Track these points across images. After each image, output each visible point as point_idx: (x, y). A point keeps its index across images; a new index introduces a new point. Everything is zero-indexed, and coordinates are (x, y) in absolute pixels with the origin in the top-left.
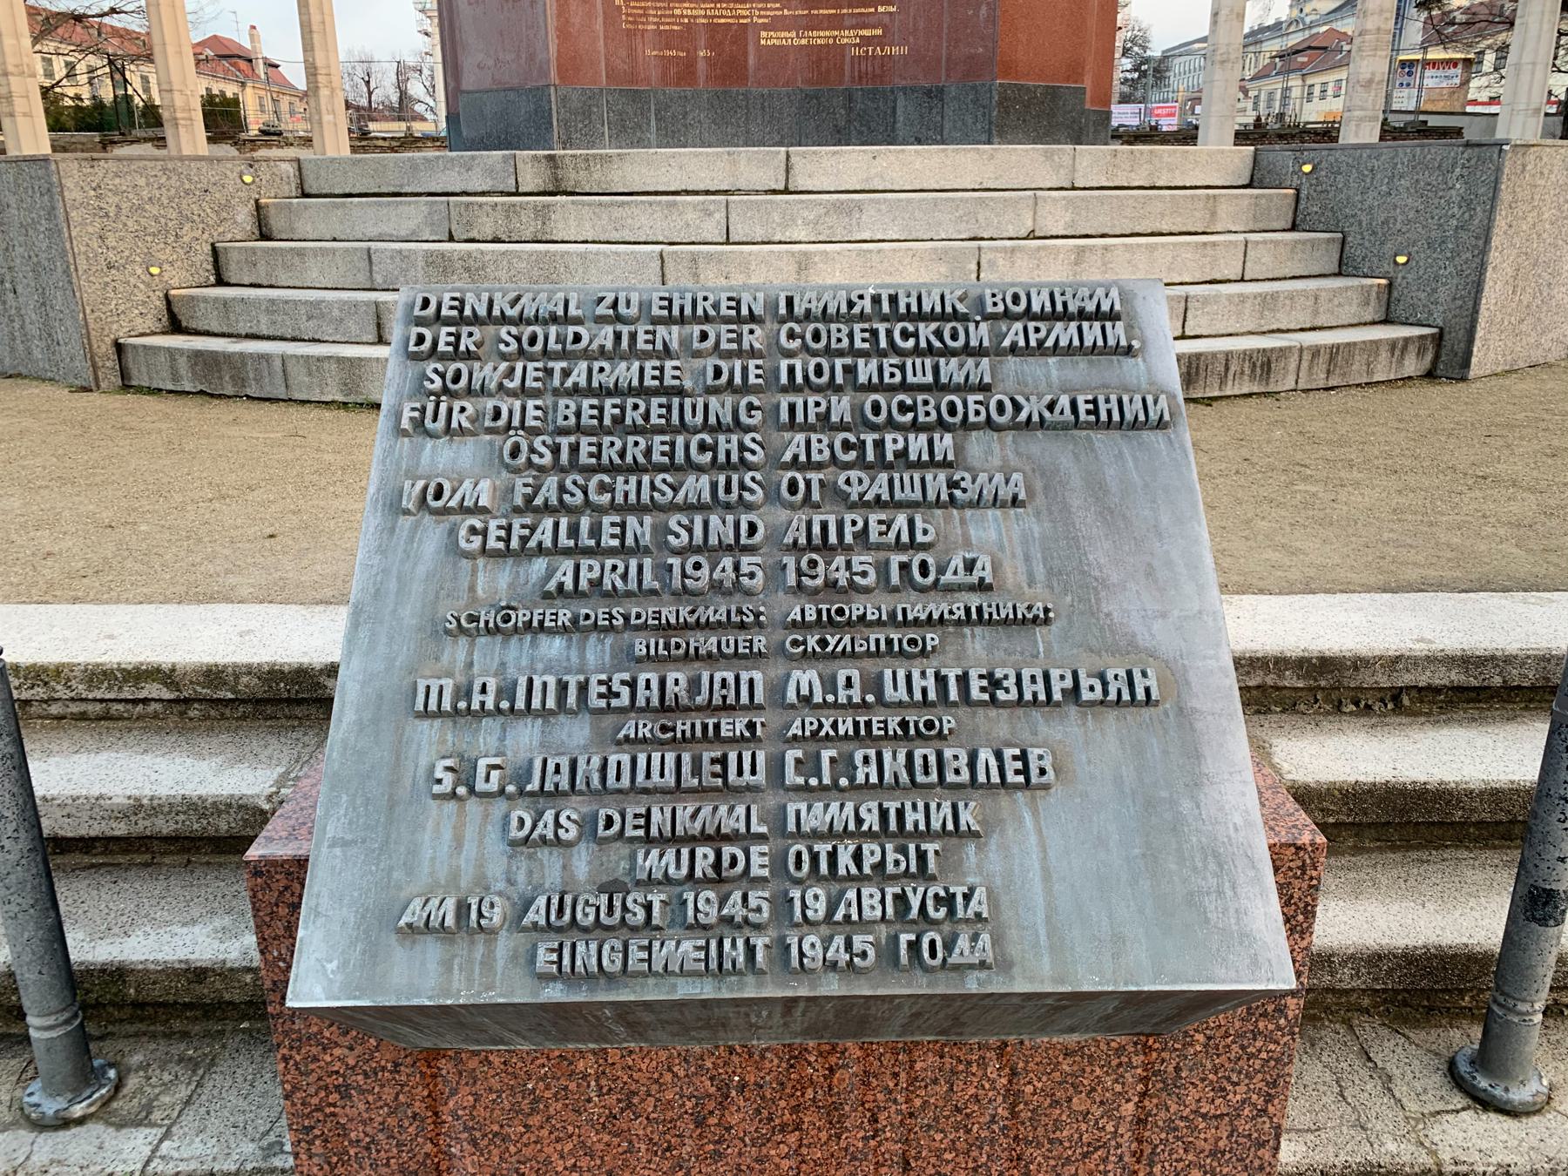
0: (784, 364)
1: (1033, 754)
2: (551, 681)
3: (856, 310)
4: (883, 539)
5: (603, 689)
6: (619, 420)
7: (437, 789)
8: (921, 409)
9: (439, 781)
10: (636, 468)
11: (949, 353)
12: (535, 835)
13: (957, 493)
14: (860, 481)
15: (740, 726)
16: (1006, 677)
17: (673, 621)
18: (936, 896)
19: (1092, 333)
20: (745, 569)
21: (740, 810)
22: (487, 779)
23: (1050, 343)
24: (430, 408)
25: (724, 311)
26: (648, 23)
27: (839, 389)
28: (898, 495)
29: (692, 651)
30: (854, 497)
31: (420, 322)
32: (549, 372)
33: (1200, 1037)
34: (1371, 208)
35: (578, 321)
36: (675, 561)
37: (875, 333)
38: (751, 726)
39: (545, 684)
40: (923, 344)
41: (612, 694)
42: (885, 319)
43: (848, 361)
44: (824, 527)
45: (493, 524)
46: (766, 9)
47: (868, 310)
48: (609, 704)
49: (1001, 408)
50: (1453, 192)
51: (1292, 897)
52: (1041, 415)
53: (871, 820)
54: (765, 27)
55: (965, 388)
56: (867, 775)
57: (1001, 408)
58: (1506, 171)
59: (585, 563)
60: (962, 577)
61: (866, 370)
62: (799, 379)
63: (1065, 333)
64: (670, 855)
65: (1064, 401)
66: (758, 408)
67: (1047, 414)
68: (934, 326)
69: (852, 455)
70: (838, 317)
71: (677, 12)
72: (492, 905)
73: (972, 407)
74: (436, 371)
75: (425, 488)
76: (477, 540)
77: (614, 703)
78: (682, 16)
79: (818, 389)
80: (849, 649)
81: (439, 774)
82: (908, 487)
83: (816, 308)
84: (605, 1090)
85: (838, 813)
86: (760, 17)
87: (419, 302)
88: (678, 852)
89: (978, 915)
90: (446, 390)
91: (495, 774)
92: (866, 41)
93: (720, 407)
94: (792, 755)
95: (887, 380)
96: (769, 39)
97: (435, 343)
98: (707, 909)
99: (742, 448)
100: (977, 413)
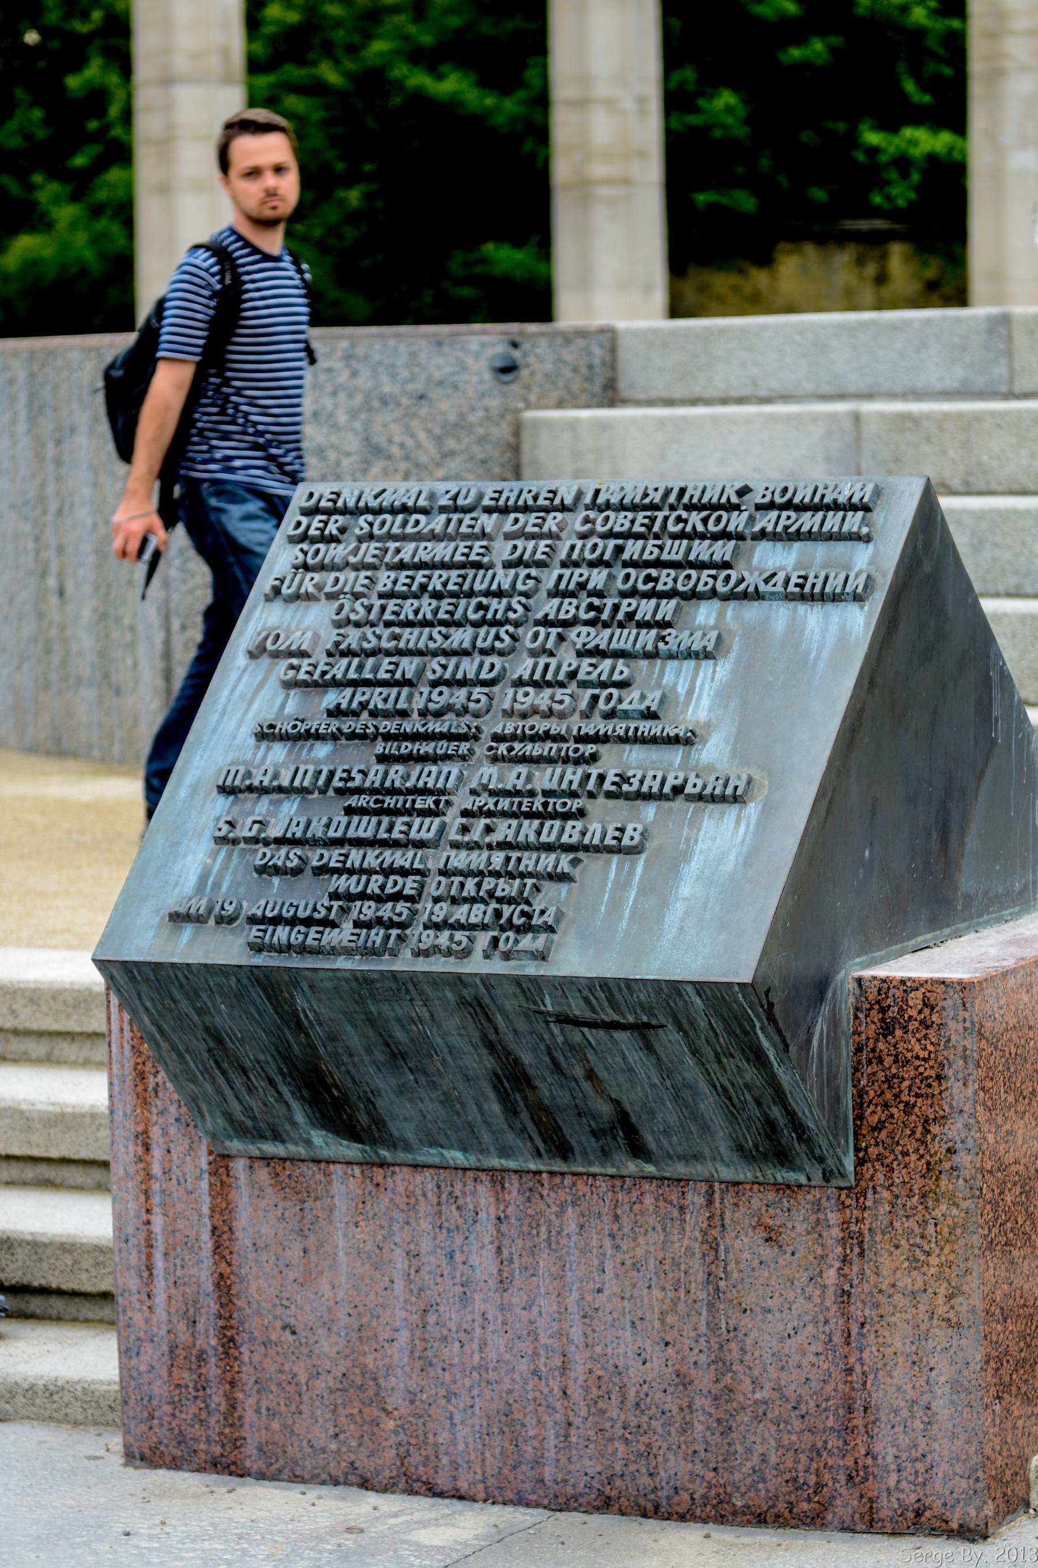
2: (311, 769)
4: (588, 678)
13: (661, 645)
43: (620, 542)
44: (547, 666)
51: (949, 1041)
52: (756, 588)
60: (636, 706)
61: (633, 549)
64: (355, 878)
65: (780, 578)
67: (762, 587)
77: (350, 784)
85: (477, 860)
91: (256, 826)
97: (308, 527)
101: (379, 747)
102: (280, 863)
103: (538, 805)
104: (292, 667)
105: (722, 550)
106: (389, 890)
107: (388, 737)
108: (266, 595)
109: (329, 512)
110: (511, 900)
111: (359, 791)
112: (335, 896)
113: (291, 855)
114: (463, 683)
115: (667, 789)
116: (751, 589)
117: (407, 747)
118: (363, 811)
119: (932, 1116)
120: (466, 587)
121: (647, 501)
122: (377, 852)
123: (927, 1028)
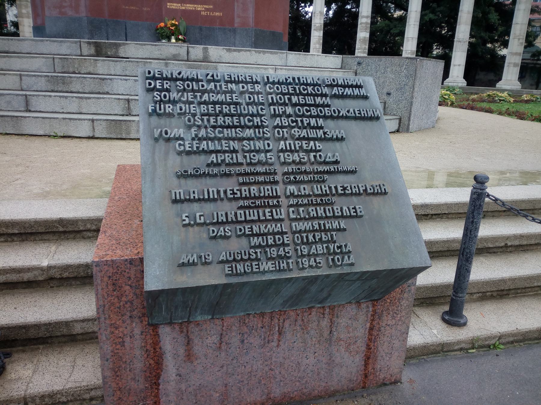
1: (357, 207)
5: (232, 192)
6: (221, 112)
7: (184, 223)
8: (312, 112)
9: (184, 220)
10: (228, 127)
11: (317, 95)
12: (219, 235)
13: (327, 135)
14: (298, 132)
15: (275, 202)
16: (347, 187)
17: (249, 172)
18: (337, 246)
19: (356, 91)
20: (269, 157)
21: (279, 225)
22: (200, 219)
23: (345, 94)
24: (158, 106)
27: (287, 105)
28: (310, 136)
29: (257, 181)
30: (297, 136)
31: (147, 78)
32: (195, 97)
34: (379, 77)
35: (202, 81)
36: (247, 154)
37: (295, 88)
38: (278, 202)
39: (213, 191)
41: (234, 193)
42: (297, 85)
45: (187, 143)
48: (234, 197)
49: (334, 111)
50: (403, 73)
53: (317, 227)
55: (324, 106)
56: (313, 214)
57: (334, 111)
58: (419, 67)
59: (219, 155)
61: (295, 99)
62: (275, 101)
63: (348, 91)
64: (260, 238)
65: (351, 110)
66: (264, 109)
67: (347, 114)
68: (312, 87)
69: (295, 124)
70: (282, 83)
72: (208, 255)
73: (327, 111)
74: (157, 94)
75: (161, 131)
76: (182, 148)
77: (236, 196)
79: (281, 105)
80: (303, 179)
81: (184, 218)
82: (312, 134)
83: (276, 81)
85: (307, 225)
87: (147, 72)
89: (349, 250)
90: (161, 101)
91: (202, 218)
92: (207, 10)
94: (291, 209)
95: (301, 102)
98: (274, 253)
99: (262, 121)
104: (180, 145)
105: (328, 101)
107: (240, 175)
110: (328, 242)
111: (241, 198)
121: (288, 81)
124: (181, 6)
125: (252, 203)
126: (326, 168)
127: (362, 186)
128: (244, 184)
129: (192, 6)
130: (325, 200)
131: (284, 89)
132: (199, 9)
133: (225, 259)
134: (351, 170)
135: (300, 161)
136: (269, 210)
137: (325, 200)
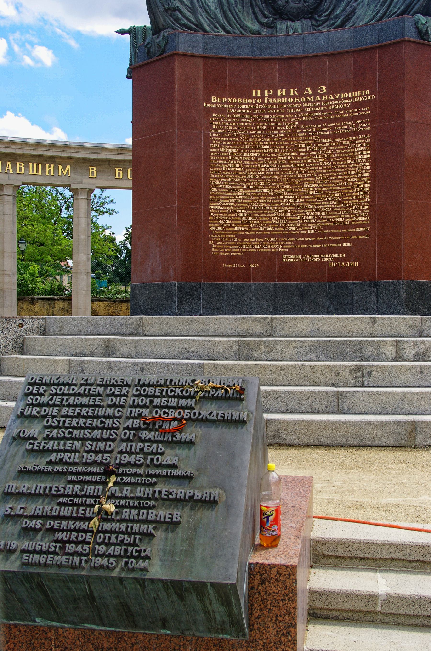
0: (132, 399)
3: (159, 383)
5: (56, 489)
8: (170, 413)
9: (7, 511)
10: (81, 428)
13: (174, 439)
14: (146, 434)
23: (215, 395)
25: (119, 383)
26: (225, 252)
31: (30, 384)
33: (261, 642)
39: (41, 487)
40: (176, 394)
43: (152, 398)
44: (131, 446)
46: (286, 245)
47: (163, 383)
51: (287, 586)
52: (206, 417)
54: (285, 253)
57: (195, 414)
61: (157, 401)
64: (65, 533)
71: (240, 246)
75: (21, 431)
76: (31, 446)
77: (59, 493)
78: (243, 248)
81: (8, 509)
84: (57, 646)
86: (282, 248)
87: (31, 378)
88: (67, 534)
91: (22, 510)
92: (336, 260)
93: (110, 411)
96: (285, 259)
97: (32, 390)
100: (187, 415)
101: (69, 477)
102: (33, 526)
103: (136, 503)
104: (30, 444)
106: (80, 539)
107: (72, 473)
108: (18, 415)
109: (40, 385)
110: (129, 544)
111: (63, 495)
112: (57, 541)
113: (37, 523)
114: (100, 452)
115: (187, 497)
116: (204, 417)
117: (80, 478)
118: (65, 504)
119: (279, 614)
120: (96, 414)
121: (159, 383)
122: (73, 522)
123: (278, 582)
124: (302, 257)
125: (71, 500)
126: (158, 471)
127: (190, 493)
128: (70, 482)
129: (316, 256)
130: (143, 503)
131: (150, 391)
132: (326, 259)
133: (26, 549)
134: (185, 475)
135: (135, 463)
136: (84, 508)
137: (143, 503)
